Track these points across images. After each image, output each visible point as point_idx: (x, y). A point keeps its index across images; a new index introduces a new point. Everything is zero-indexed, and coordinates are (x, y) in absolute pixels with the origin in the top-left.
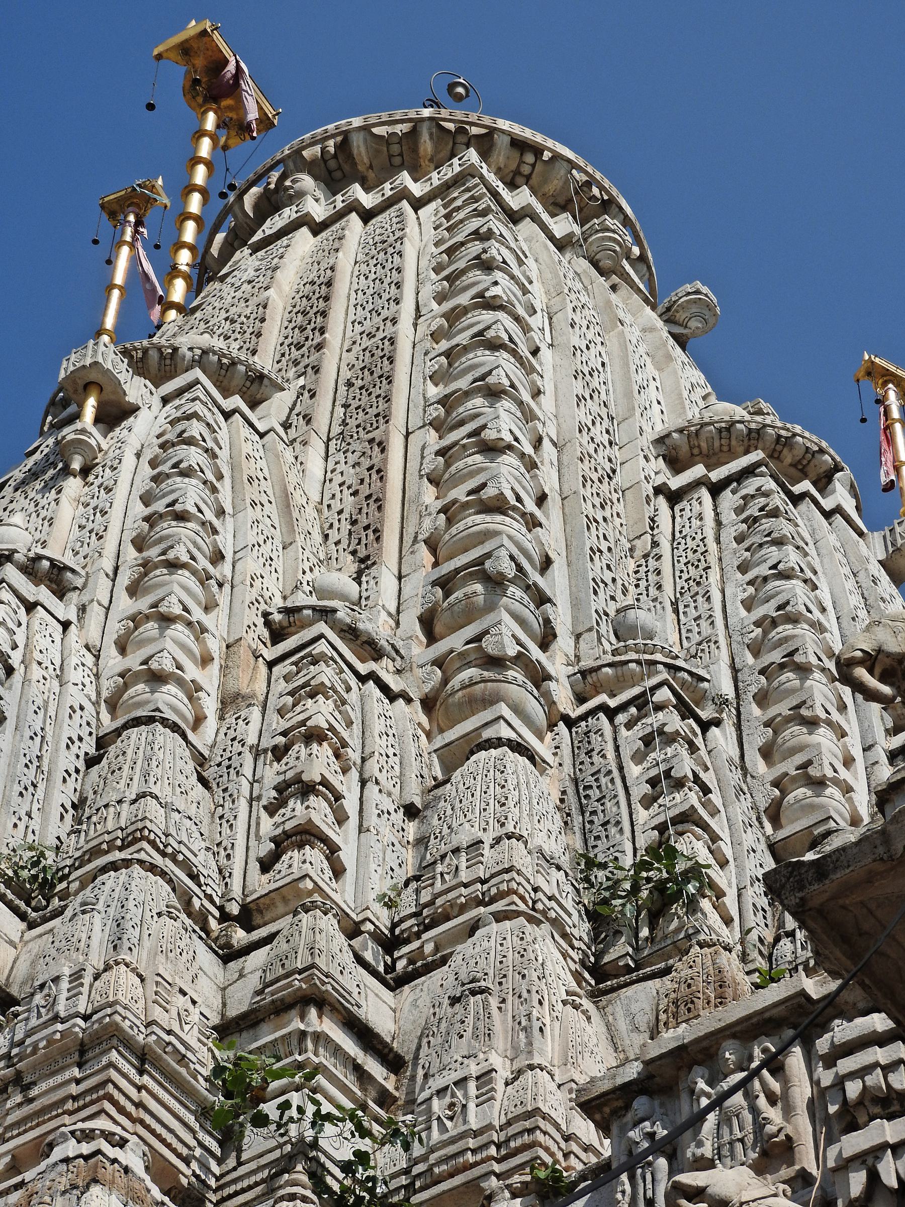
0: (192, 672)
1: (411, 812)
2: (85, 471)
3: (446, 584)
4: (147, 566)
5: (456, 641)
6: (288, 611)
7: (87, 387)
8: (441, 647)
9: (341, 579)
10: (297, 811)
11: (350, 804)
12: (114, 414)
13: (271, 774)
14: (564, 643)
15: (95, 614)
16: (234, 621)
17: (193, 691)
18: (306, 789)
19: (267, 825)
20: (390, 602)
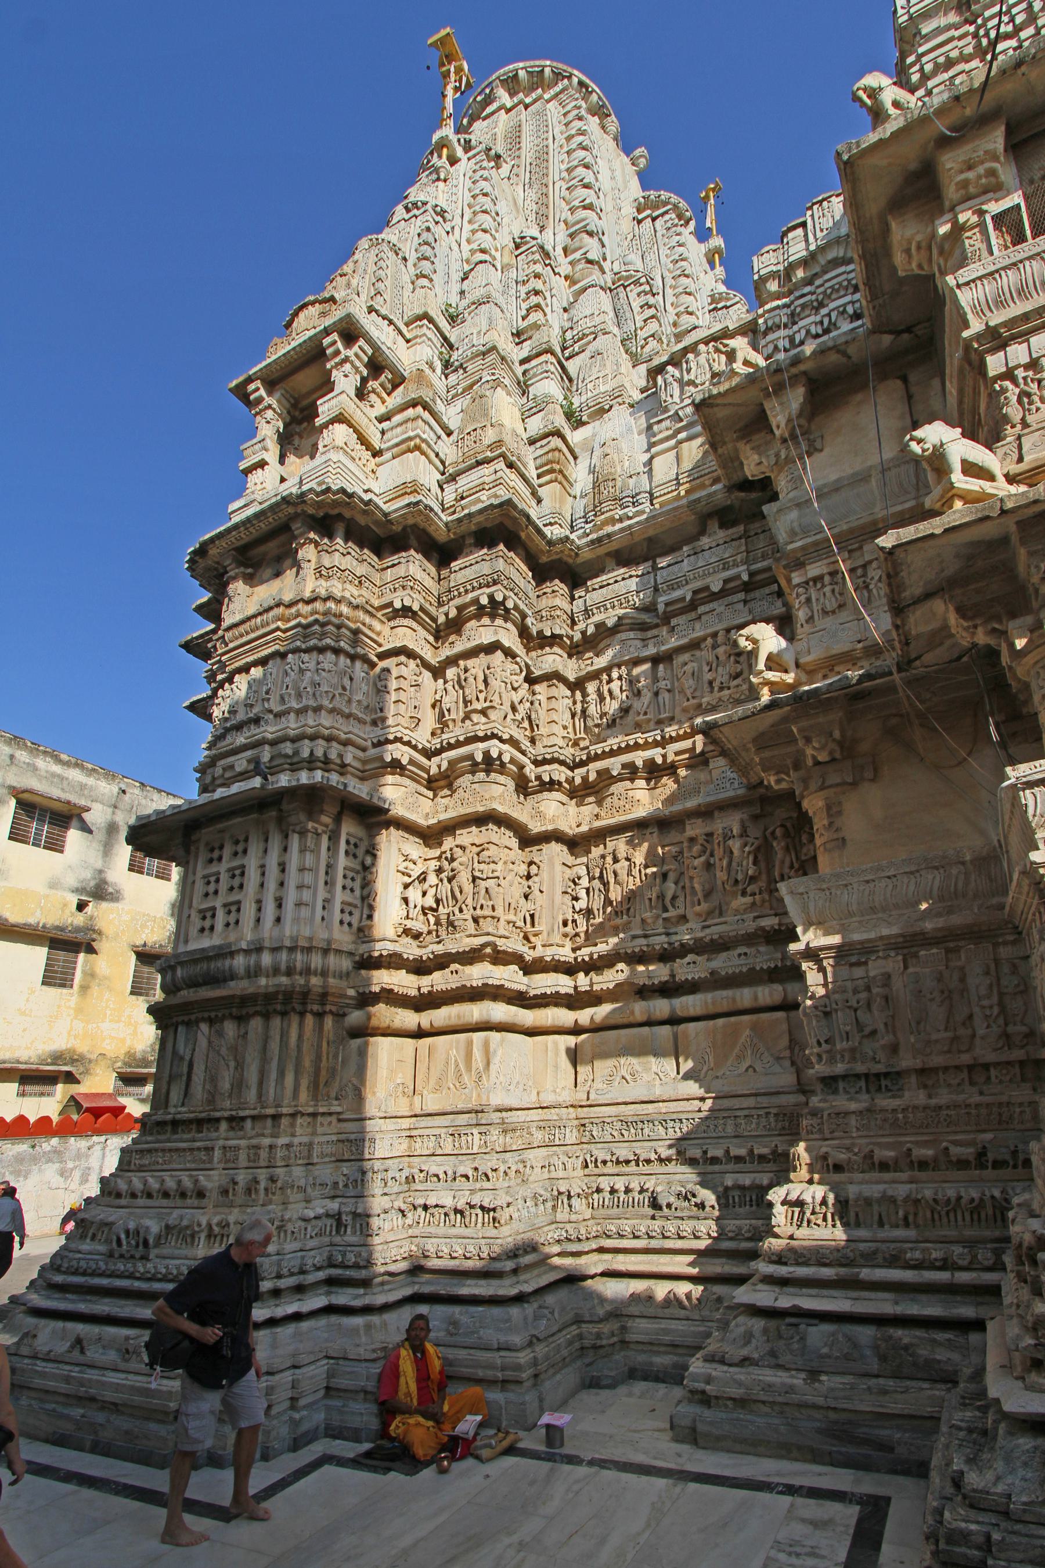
0: (493, 252)
1: (565, 310)
2: (445, 181)
3: (572, 236)
4: (475, 213)
5: (577, 255)
6: (522, 238)
7: (443, 147)
8: (570, 258)
9: (534, 232)
10: (534, 300)
11: (549, 300)
12: (453, 161)
13: (523, 290)
14: (608, 262)
15: (457, 230)
16: (505, 239)
17: (495, 259)
18: (537, 293)
19: (525, 306)
20: (554, 238)
